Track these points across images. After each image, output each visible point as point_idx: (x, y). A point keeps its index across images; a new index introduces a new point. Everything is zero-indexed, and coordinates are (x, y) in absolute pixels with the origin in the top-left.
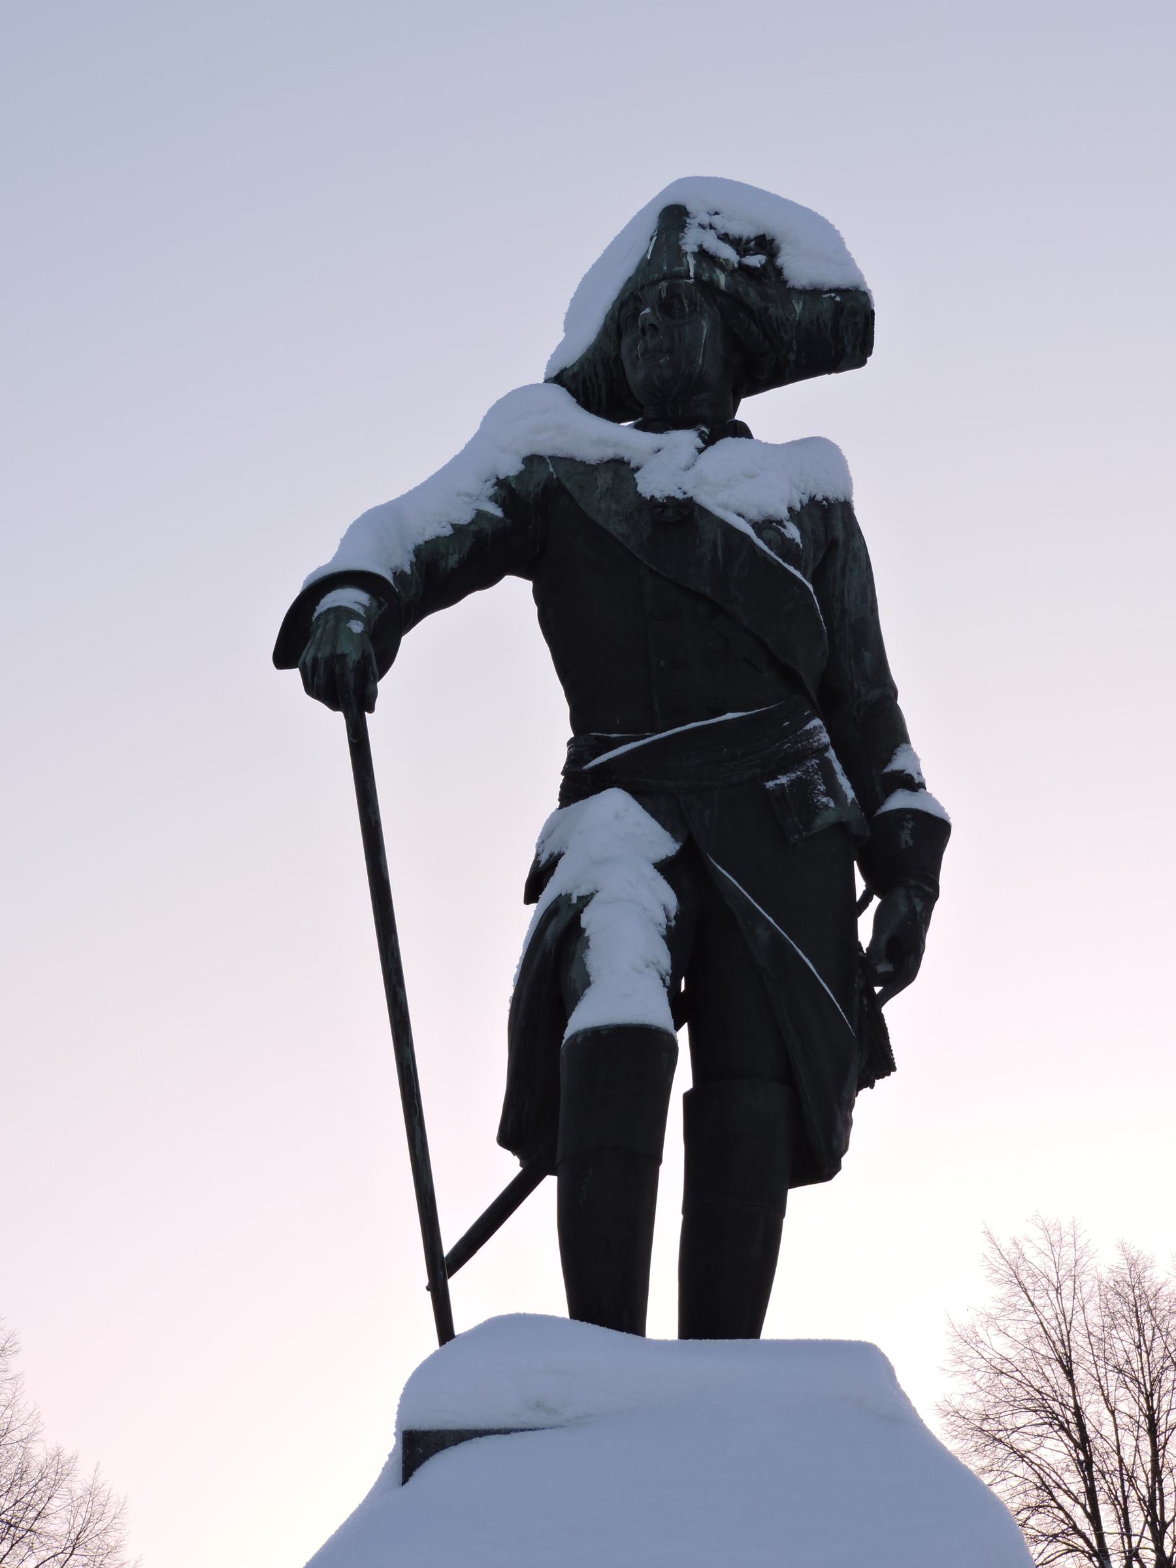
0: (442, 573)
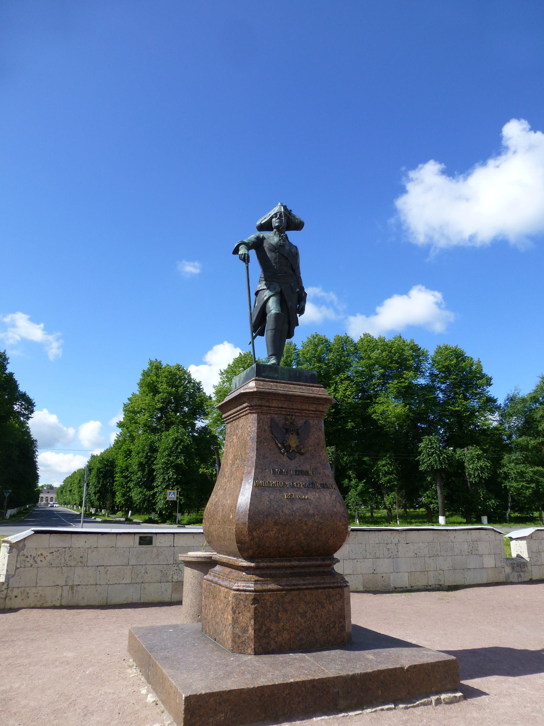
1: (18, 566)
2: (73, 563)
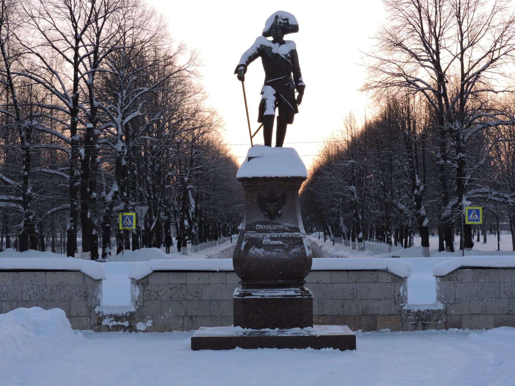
0: (251, 59)
1: (145, 299)
2: (190, 298)
